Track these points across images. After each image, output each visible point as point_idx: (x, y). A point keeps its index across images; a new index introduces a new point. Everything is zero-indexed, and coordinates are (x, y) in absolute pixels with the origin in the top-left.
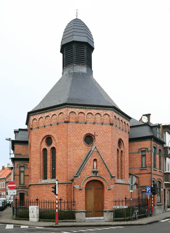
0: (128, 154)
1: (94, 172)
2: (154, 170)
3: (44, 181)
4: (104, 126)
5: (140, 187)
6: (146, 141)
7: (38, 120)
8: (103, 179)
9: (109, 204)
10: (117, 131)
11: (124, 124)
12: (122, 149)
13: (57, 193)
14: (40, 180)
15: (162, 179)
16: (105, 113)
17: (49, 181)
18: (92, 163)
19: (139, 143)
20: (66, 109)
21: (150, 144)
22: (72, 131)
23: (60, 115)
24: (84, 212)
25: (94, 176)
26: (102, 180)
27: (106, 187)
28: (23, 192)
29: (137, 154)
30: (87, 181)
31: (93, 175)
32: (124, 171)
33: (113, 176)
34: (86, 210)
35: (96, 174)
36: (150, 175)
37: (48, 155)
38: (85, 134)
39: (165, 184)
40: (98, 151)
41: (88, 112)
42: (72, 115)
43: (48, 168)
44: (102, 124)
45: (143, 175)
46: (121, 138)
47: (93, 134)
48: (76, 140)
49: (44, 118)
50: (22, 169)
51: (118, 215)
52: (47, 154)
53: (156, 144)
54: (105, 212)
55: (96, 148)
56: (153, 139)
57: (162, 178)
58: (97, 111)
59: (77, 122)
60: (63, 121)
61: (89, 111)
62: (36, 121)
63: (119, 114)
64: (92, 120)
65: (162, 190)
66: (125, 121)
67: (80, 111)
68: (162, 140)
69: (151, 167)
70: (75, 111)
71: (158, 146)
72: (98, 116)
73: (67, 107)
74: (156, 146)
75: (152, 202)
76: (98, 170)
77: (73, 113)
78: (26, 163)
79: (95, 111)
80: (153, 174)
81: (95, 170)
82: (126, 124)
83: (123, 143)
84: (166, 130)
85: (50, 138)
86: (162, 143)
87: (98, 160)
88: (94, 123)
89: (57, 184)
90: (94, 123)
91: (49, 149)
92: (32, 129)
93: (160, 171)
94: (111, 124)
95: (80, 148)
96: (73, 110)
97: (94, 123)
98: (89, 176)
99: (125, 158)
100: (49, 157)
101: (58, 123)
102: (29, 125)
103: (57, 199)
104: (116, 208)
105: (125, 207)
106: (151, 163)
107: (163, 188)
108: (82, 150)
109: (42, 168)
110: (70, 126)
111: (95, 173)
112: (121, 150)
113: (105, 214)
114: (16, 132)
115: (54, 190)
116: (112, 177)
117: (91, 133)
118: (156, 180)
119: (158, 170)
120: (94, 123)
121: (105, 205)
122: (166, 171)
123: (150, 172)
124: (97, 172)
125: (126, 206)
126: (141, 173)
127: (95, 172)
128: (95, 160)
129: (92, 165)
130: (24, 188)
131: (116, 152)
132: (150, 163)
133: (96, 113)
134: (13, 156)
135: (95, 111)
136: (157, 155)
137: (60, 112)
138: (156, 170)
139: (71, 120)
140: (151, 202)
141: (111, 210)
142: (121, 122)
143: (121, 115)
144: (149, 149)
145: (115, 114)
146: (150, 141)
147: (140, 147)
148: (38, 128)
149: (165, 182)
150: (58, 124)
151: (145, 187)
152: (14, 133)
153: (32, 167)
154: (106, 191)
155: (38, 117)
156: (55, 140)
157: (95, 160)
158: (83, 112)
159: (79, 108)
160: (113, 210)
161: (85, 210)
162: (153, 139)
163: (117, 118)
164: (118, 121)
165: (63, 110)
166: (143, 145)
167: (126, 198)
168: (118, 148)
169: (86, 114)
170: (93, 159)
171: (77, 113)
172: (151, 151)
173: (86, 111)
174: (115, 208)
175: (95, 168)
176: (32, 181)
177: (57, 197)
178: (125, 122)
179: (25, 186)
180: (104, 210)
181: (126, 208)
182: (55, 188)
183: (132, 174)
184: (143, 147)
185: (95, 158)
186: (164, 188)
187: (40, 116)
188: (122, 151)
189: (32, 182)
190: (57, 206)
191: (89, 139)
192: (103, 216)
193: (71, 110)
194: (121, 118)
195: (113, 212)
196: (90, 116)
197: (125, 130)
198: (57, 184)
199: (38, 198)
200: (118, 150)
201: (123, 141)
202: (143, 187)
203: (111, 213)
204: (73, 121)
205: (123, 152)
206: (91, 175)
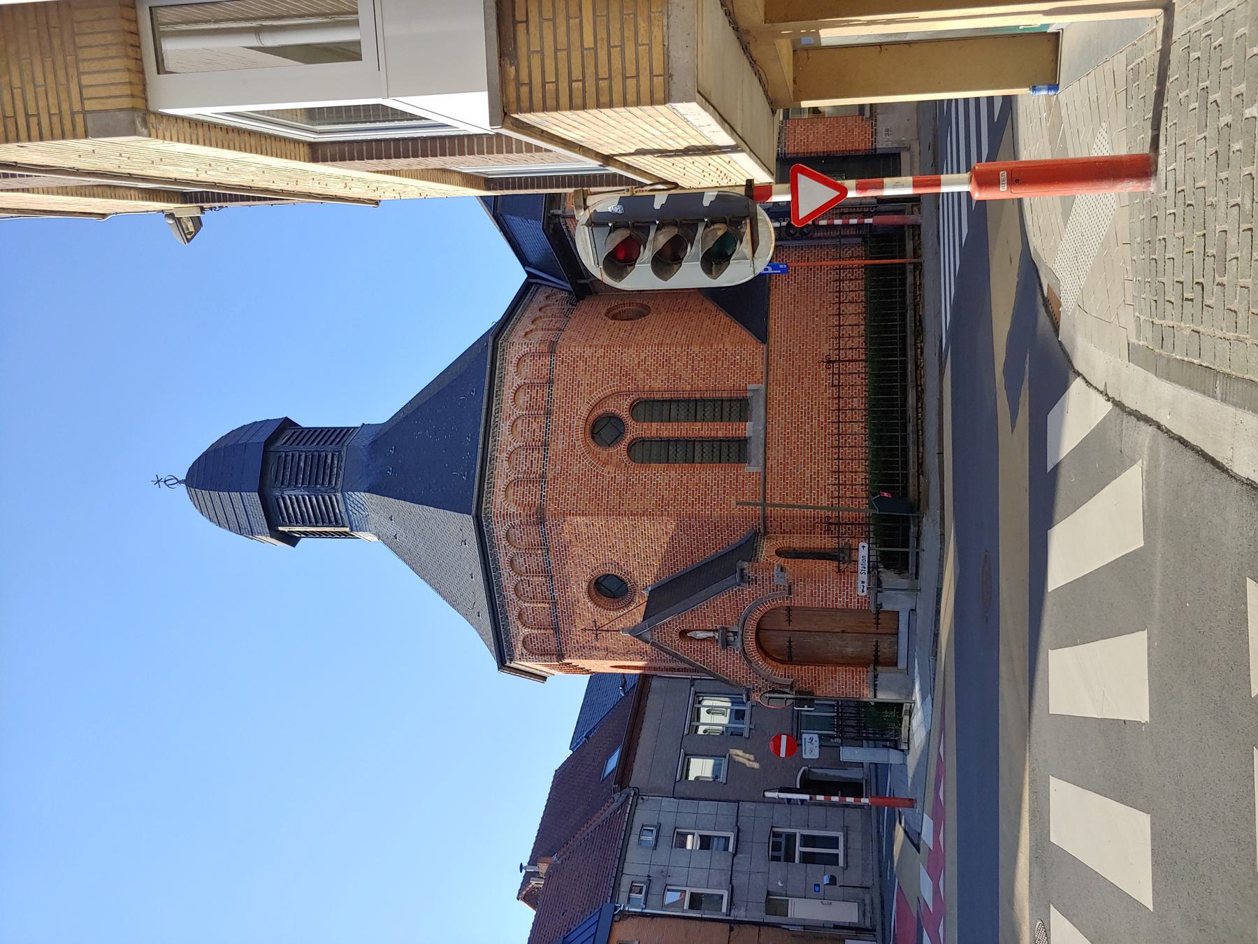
18: (695, 646)
26: (757, 615)
31: (739, 645)
34: (867, 666)
35: (735, 633)
46: (581, 423)
56: (560, 212)
58: (505, 571)
61: (510, 594)
113: (886, 607)
121: (854, 605)
154: (798, 602)
157: (683, 634)
168: (623, 446)
170: (678, 642)
175: (711, 634)
185: (675, 636)
205: (634, 396)
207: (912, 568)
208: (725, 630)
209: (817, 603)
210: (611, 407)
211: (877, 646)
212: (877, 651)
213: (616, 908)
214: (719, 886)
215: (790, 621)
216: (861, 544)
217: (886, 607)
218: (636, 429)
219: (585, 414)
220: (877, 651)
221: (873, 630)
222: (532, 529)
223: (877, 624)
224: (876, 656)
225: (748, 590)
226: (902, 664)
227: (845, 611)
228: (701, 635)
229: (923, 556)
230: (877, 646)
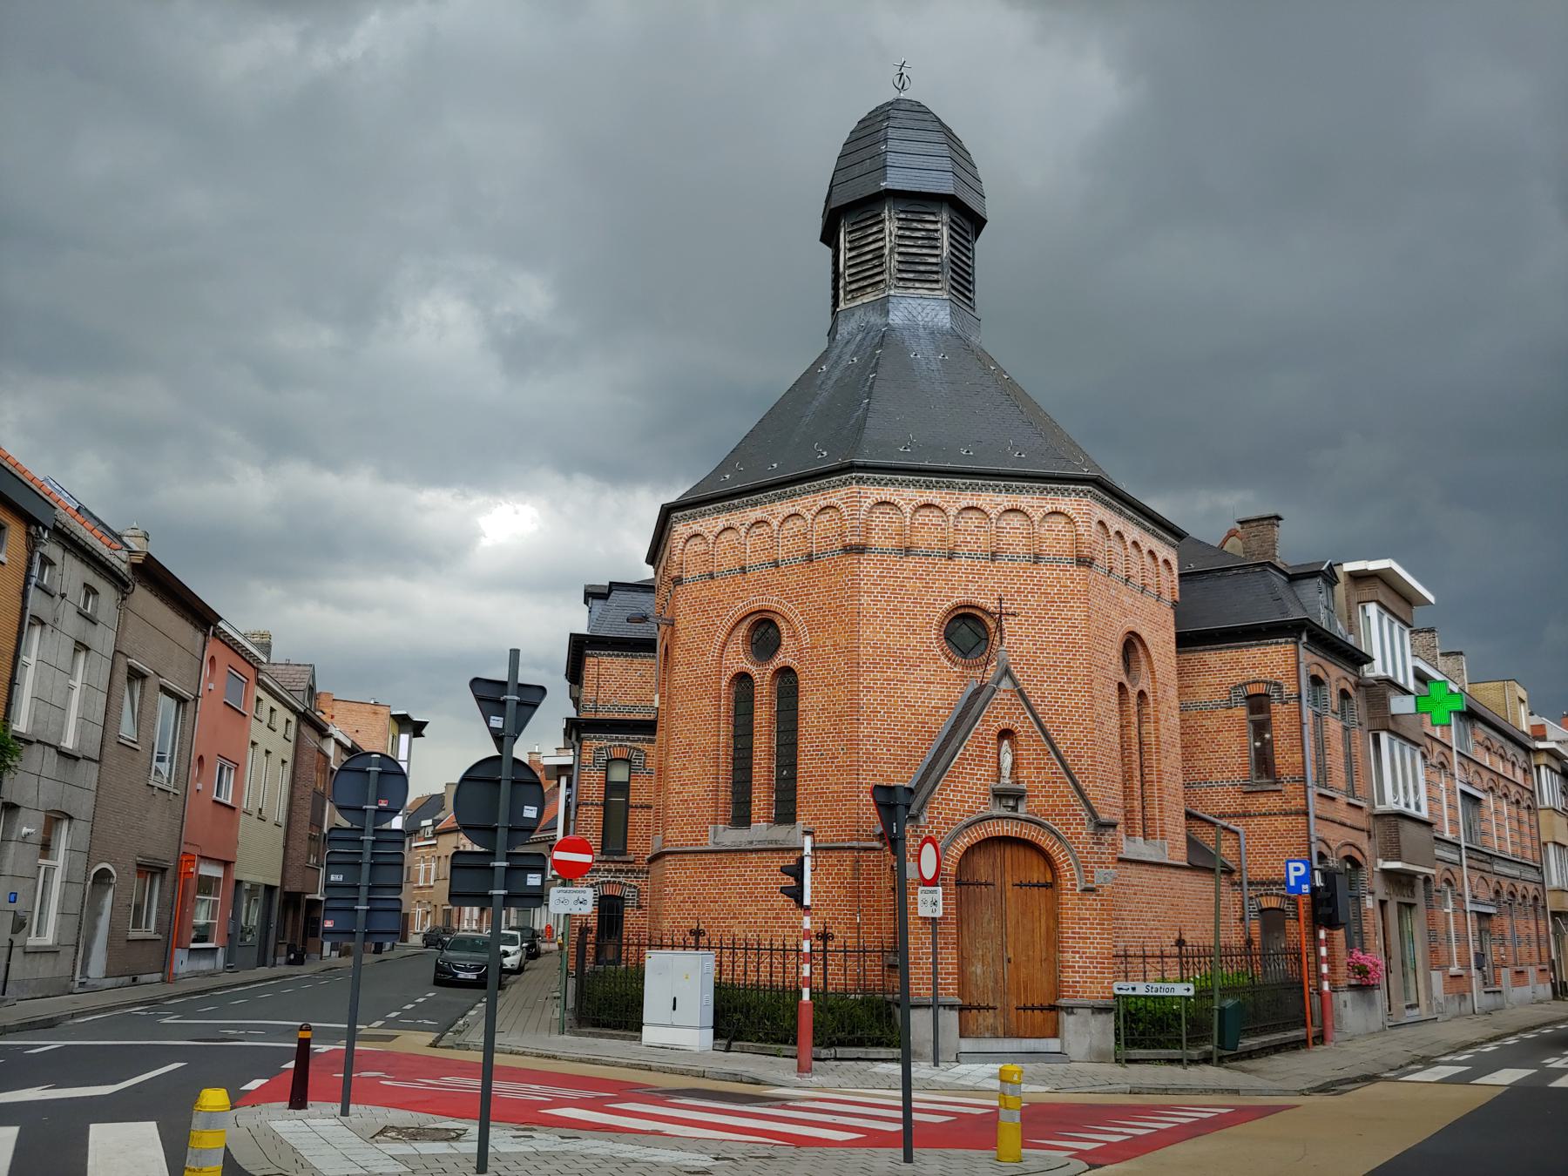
0: (1176, 712)
1: (1000, 795)
2: (1320, 795)
3: (733, 837)
4: (1044, 570)
5: (1250, 883)
6: (1268, 649)
7: (711, 538)
8: (1053, 832)
9: (1087, 970)
10: (1114, 592)
11: (1148, 559)
12: (1144, 684)
13: (807, 902)
14: (715, 831)
15: (1365, 844)
16: (1049, 508)
17: (761, 831)
19: (1228, 655)
20: (855, 488)
21: (1292, 661)
22: (883, 592)
23: (823, 518)
24: (952, 1007)
25: (999, 818)
26: (1045, 841)
27: (1071, 878)
28: (617, 893)
29: (1222, 713)
30: (964, 842)
31: (995, 812)
32: (1161, 799)
33: (1104, 817)
35: (1015, 809)
36: (1301, 819)
37: (757, 704)
38: (948, 605)
39: (1384, 871)
40: (1021, 692)
41: (964, 504)
42: (879, 518)
43: (756, 769)
44: (1037, 559)
45: (1264, 822)
47: (991, 605)
48: (902, 635)
49: (743, 530)
50: (619, 774)
51: (1144, 1029)
52: (751, 698)
53: (1322, 661)
54: (1070, 1010)
55: (1012, 678)
57: (1362, 840)
59: (908, 551)
60: (839, 545)
61: (967, 499)
62: (703, 547)
63: (1121, 513)
64: (984, 542)
65: (1369, 903)
66: (1154, 549)
67: (923, 500)
68: (1351, 640)
69: (1304, 780)
70: (895, 498)
71: (1336, 675)
72: (1016, 520)
73: (859, 481)
74: (1322, 675)
75: (1325, 969)
76: (1024, 786)
77: (887, 509)
78: (639, 745)
79: (999, 500)
80: (1317, 817)
81: (1006, 782)
82: (1160, 560)
83: (1148, 656)
84: (1366, 592)
85: (772, 623)
86: (1357, 659)
87: (1021, 738)
88: (994, 556)
89: (808, 850)
90: (993, 554)
91: (762, 675)
92: (678, 581)
93: (1352, 801)
94: (1085, 562)
95: (924, 672)
96: (887, 493)
97: (993, 554)
98: (974, 817)
99: (1163, 731)
100: (763, 715)
101: (810, 555)
102: (664, 563)
103: (807, 935)
104: (1130, 992)
105: (1180, 990)
106: (1304, 762)
107: (1372, 893)
108: (937, 685)
109: (726, 767)
110: (867, 566)
111: (1011, 803)
112: (1137, 690)
113: (1068, 1022)
114: (593, 595)
115: (791, 882)
116: (1103, 826)
117: (980, 601)
118: (1334, 847)
119: (1342, 800)
120: (994, 556)
121: (1069, 977)
122: (1382, 800)
123: (1298, 803)
124: (1018, 796)
125: (1186, 985)
126: (1252, 809)
127: (1009, 797)
128: (1006, 734)
129: (993, 762)
130: (621, 871)
131: (1115, 700)
132: (1298, 757)
133: (1001, 509)
134: (573, 714)
135: (999, 500)
136: (1331, 720)
137: (823, 503)
138: (1333, 799)
139: (876, 540)
140: (1318, 969)
141: (1100, 1003)
142: (1134, 551)
143: (1130, 519)
144: (1289, 688)
145: (1101, 512)
146: (1289, 647)
147: (1235, 677)
148: (711, 576)
149: (1380, 861)
150: (810, 558)
151: (1275, 883)
152: (586, 602)
153: (674, 763)
154: (1070, 901)
155: (710, 523)
156: (794, 636)
157: (1006, 734)
158: (936, 501)
159: (915, 484)
160: (1111, 1003)
161: (958, 1001)
162: (1305, 639)
163: (1112, 533)
164: (1118, 548)
165: (836, 496)
166: (1254, 667)
167: (1180, 943)
169: (953, 512)
170: (996, 727)
171: (908, 510)
172: (1300, 697)
173: (952, 499)
174: (1123, 992)
175: (1006, 773)
176: (670, 834)
177: (807, 923)
178: (1151, 552)
179: (631, 858)
180: (1063, 1002)
181: (1186, 993)
182: (797, 872)
183: (1198, 813)
184: (1254, 674)
185: (1005, 723)
186: (1380, 894)
187: (722, 521)
188: (1142, 694)
189: (676, 837)
190: (806, 970)
191: (968, 630)
192: (1055, 1035)
193: (874, 493)
194: (1133, 532)
195: (1112, 1016)
196: (974, 518)
197: (1154, 591)
198: (808, 850)
199: (702, 926)
200: (1121, 686)
201: (1149, 646)
202: (1263, 884)
203: (1102, 1017)
204: (890, 544)
206: (988, 813)
207: (1137, 1053)
208: (1018, 796)
209: (1068, 928)
210: (1144, 667)
211: (988, 1008)
212: (979, 1008)
213: (45, 528)
214: (35, 720)
215: (1020, 885)
216: (1191, 986)
217: (1068, 1022)
218: (1133, 693)
219: (1144, 635)
220: (979, 1008)
221: (1015, 1003)
222: (1066, 547)
223: (1025, 1009)
224: (970, 1008)
225: (1086, 832)
226: (967, 1045)
227: (1055, 967)
228: (1007, 760)
229: (1178, 1069)
230: (988, 1008)
